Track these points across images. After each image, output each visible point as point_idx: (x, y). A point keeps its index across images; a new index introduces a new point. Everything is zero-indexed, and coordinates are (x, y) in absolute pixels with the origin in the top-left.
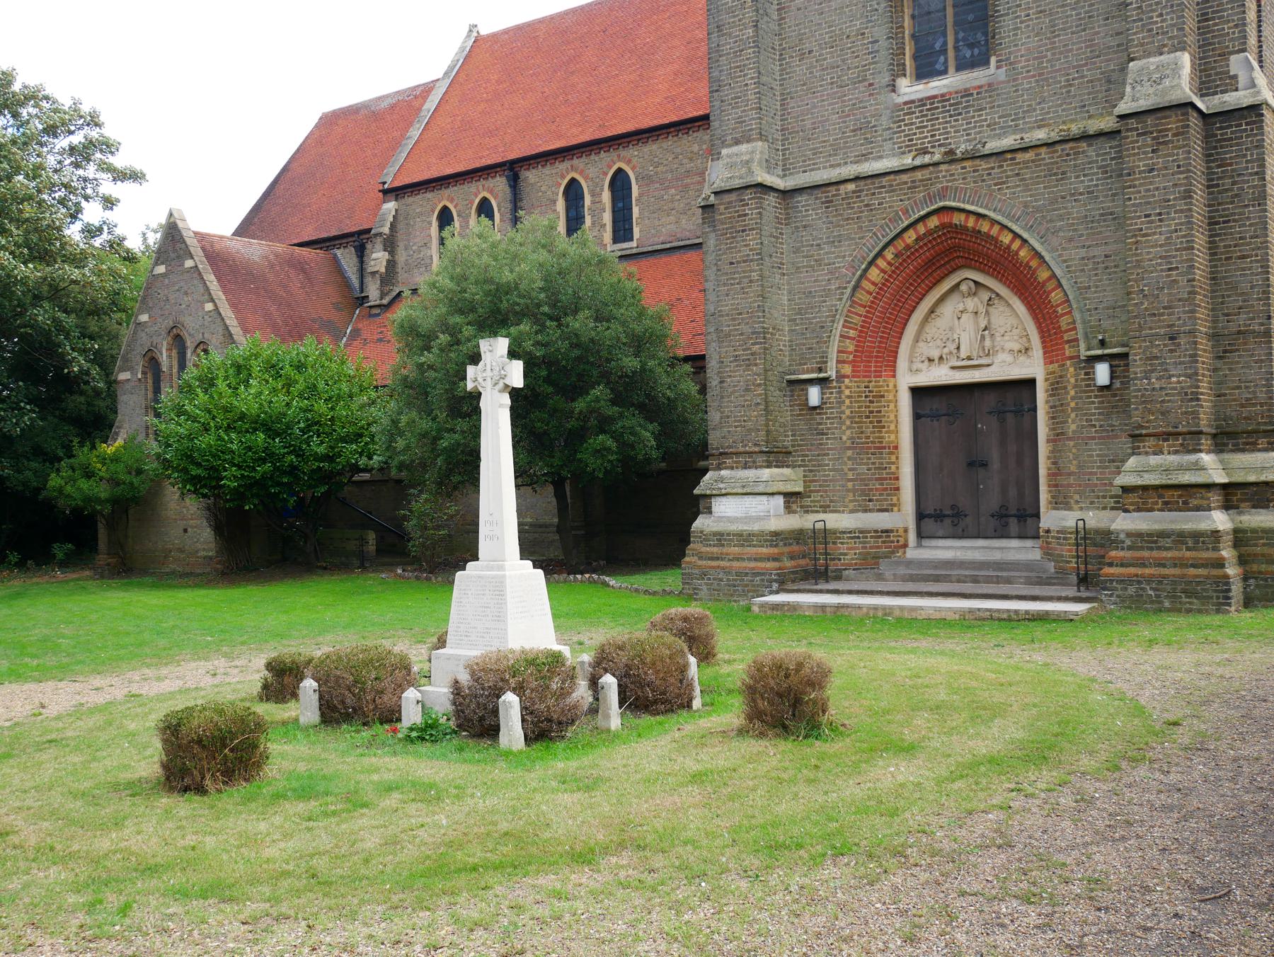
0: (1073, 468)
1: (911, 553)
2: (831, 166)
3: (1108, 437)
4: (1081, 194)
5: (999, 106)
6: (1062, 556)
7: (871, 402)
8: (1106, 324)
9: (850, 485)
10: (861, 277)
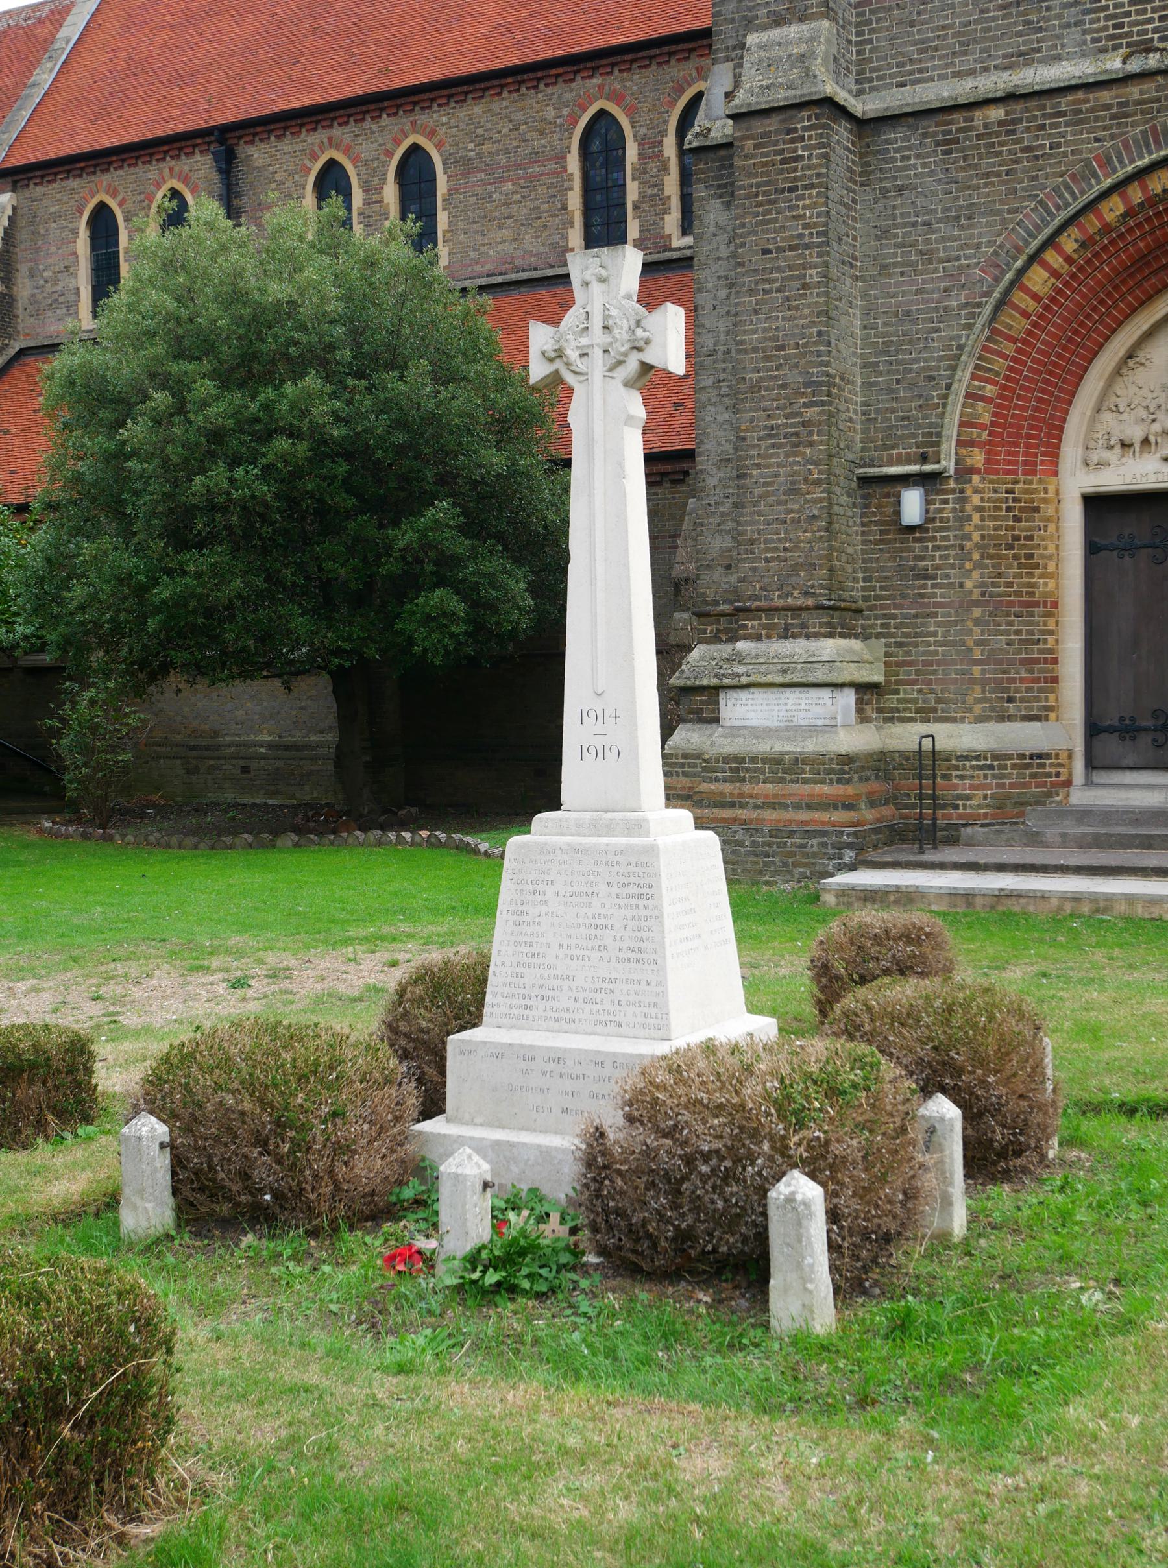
1: (1079, 797)
2: (956, 75)
7: (1017, 519)
9: (977, 670)
10: (1012, 283)
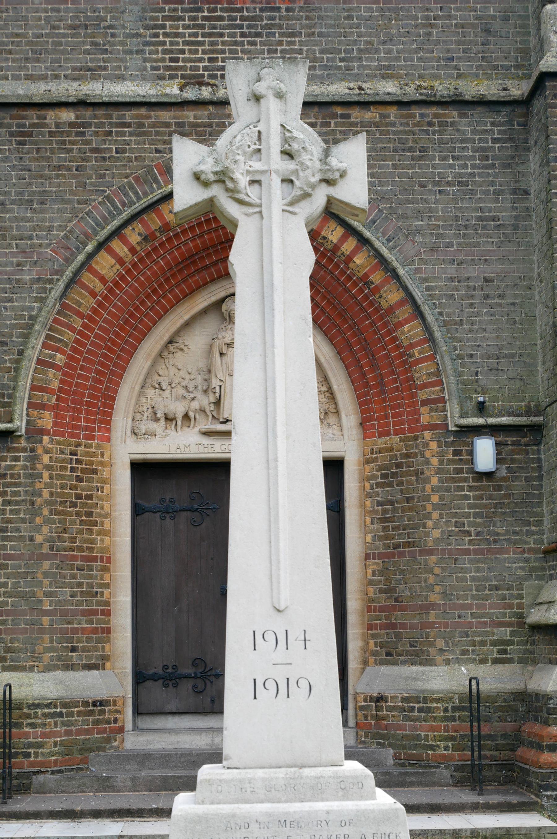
0: (434, 598)
1: (132, 742)
2: (29, 77)
3: (489, 551)
4: (449, 184)
5: (321, 34)
6: (418, 738)
7: (79, 479)
8: (485, 379)
9: (46, 620)
10: (82, 265)
